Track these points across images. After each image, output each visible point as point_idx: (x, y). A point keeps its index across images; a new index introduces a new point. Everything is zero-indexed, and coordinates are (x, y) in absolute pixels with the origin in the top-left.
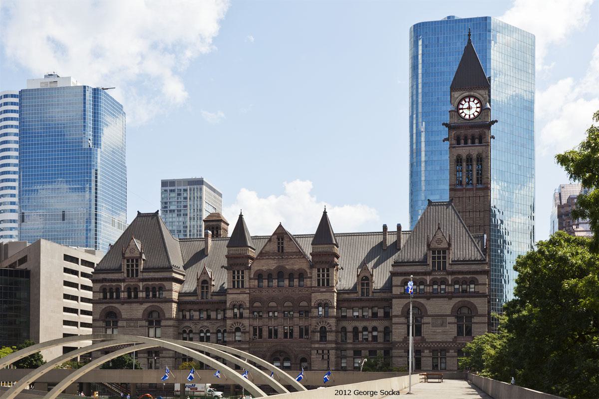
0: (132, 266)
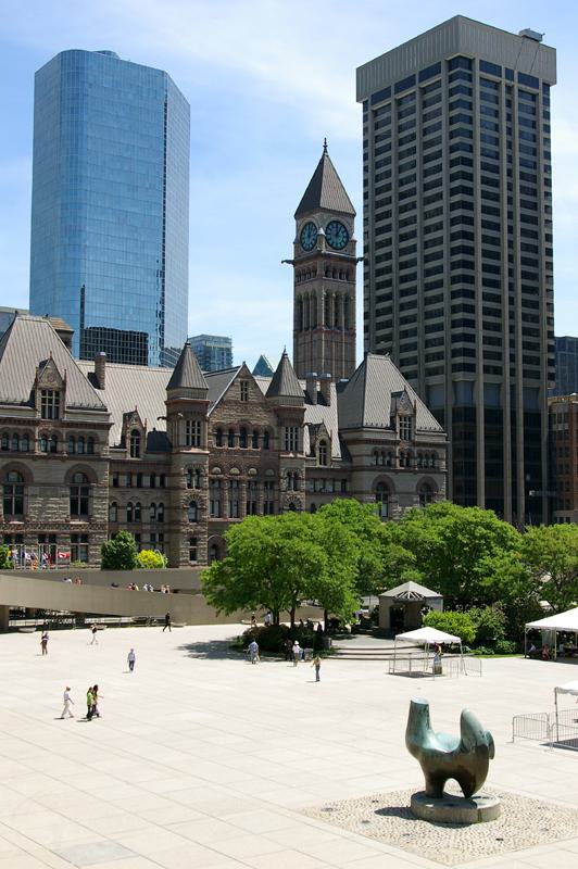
0: (50, 401)
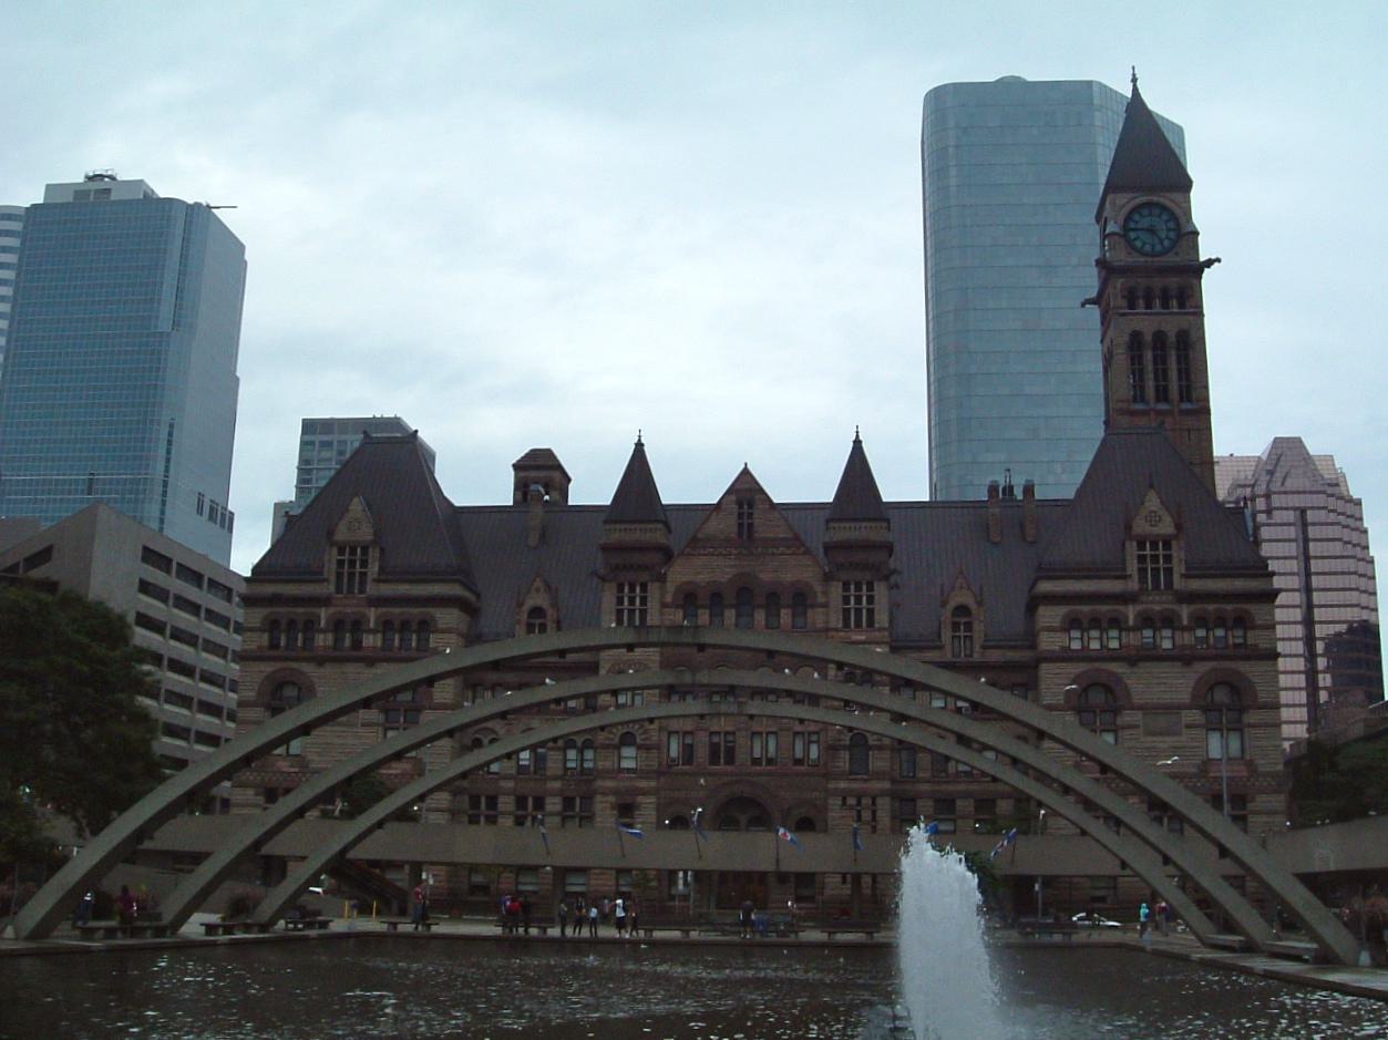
0: (352, 563)
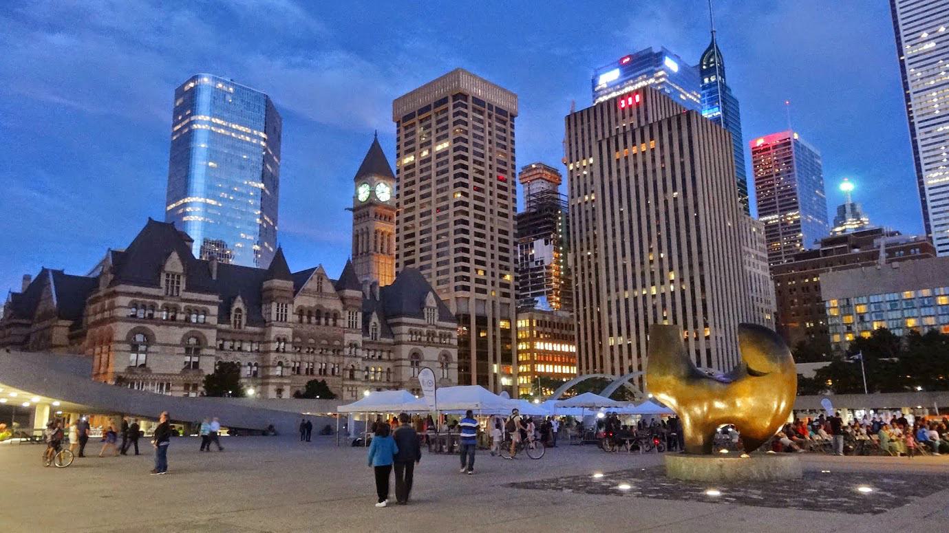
0: (173, 282)
